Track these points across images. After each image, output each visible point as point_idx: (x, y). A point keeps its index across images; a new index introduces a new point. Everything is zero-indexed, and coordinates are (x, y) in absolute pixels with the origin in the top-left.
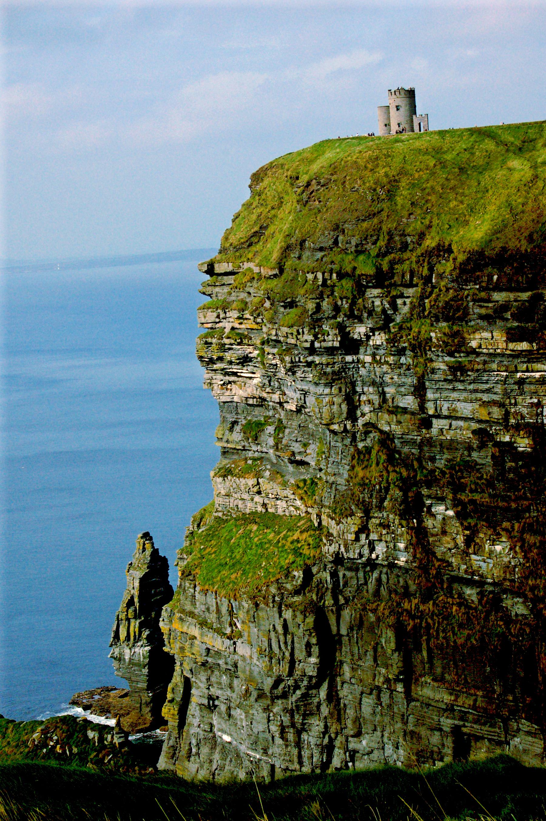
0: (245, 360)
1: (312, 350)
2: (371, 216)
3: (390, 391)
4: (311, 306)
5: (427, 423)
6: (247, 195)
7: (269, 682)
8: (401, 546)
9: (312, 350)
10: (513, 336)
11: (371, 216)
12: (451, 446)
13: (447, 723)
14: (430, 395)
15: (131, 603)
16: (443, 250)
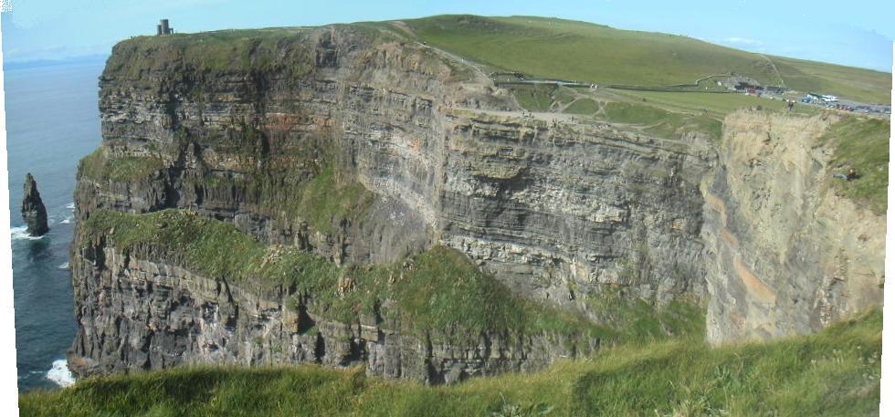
0: (120, 108)
1: (159, 102)
2: (177, 60)
3: (187, 114)
4: (158, 89)
5: (202, 123)
6: (110, 53)
7: (148, 208)
8: (194, 161)
9: (159, 102)
10: (235, 96)
11: (177, 60)
12: (212, 131)
13: (213, 213)
14: (203, 115)
15: (28, 197)
16: (208, 70)
